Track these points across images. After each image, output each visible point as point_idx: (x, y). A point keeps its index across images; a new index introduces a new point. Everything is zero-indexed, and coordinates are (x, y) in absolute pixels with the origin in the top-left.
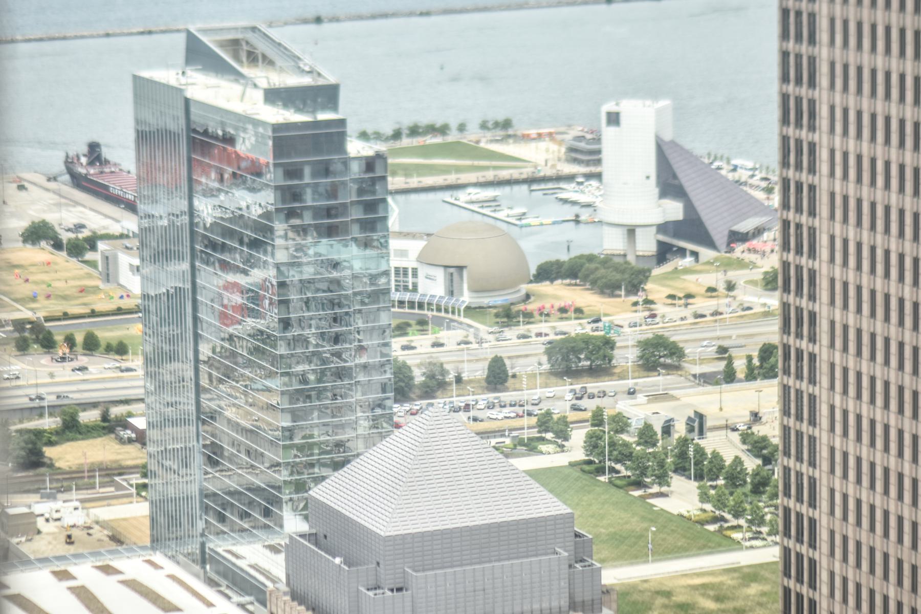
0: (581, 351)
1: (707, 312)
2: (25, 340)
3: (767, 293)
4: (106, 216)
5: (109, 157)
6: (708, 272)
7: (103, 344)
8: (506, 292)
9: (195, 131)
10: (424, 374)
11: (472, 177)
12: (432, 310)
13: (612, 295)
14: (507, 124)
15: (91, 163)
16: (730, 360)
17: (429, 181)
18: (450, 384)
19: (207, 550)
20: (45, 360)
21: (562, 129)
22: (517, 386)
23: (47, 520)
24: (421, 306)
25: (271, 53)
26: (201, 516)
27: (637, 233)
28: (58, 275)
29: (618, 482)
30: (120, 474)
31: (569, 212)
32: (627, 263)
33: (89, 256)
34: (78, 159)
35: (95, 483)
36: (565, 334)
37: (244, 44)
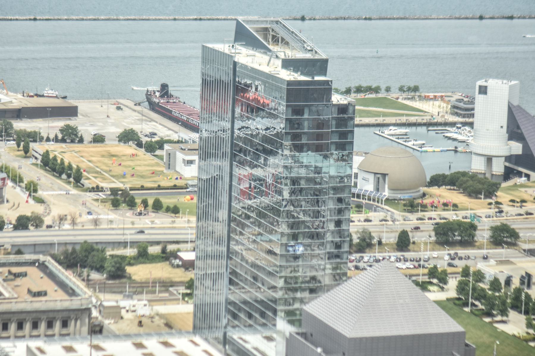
0: (455, 231)
2: (117, 201)
4: (170, 129)
5: (173, 93)
7: (165, 206)
8: (411, 191)
9: (239, 82)
10: (359, 238)
11: (393, 120)
12: (366, 199)
13: (477, 198)
14: (416, 89)
15: (162, 96)
18: (374, 245)
19: (227, 337)
20: (129, 213)
21: (450, 94)
22: (415, 249)
23: (127, 311)
24: (358, 196)
25: (287, 38)
26: (225, 317)
27: (493, 160)
28: (138, 163)
29: (476, 312)
30: (172, 286)
31: (451, 146)
32: (486, 178)
33: (158, 152)
34: (155, 93)
35: (156, 291)
36: (445, 219)
37: (271, 31)
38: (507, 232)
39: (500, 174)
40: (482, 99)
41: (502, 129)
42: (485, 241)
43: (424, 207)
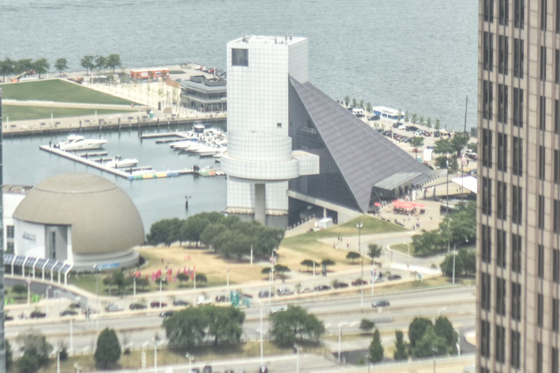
0: (205, 325)
1: (349, 281)
3: (418, 260)
6: (350, 234)
8: (117, 255)
10: (22, 349)
11: (73, 122)
14: (114, 61)
16: (376, 336)
17: (34, 125)
18: (53, 361)
21: (177, 68)
24: (18, 270)
31: (186, 164)
32: (255, 223)
36: (185, 303)
38: (302, 322)
39: (281, 213)
40: (240, 74)
41: (279, 129)
42: (261, 340)
43: (143, 285)
